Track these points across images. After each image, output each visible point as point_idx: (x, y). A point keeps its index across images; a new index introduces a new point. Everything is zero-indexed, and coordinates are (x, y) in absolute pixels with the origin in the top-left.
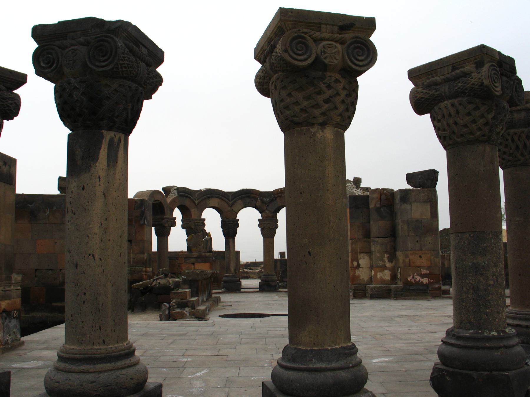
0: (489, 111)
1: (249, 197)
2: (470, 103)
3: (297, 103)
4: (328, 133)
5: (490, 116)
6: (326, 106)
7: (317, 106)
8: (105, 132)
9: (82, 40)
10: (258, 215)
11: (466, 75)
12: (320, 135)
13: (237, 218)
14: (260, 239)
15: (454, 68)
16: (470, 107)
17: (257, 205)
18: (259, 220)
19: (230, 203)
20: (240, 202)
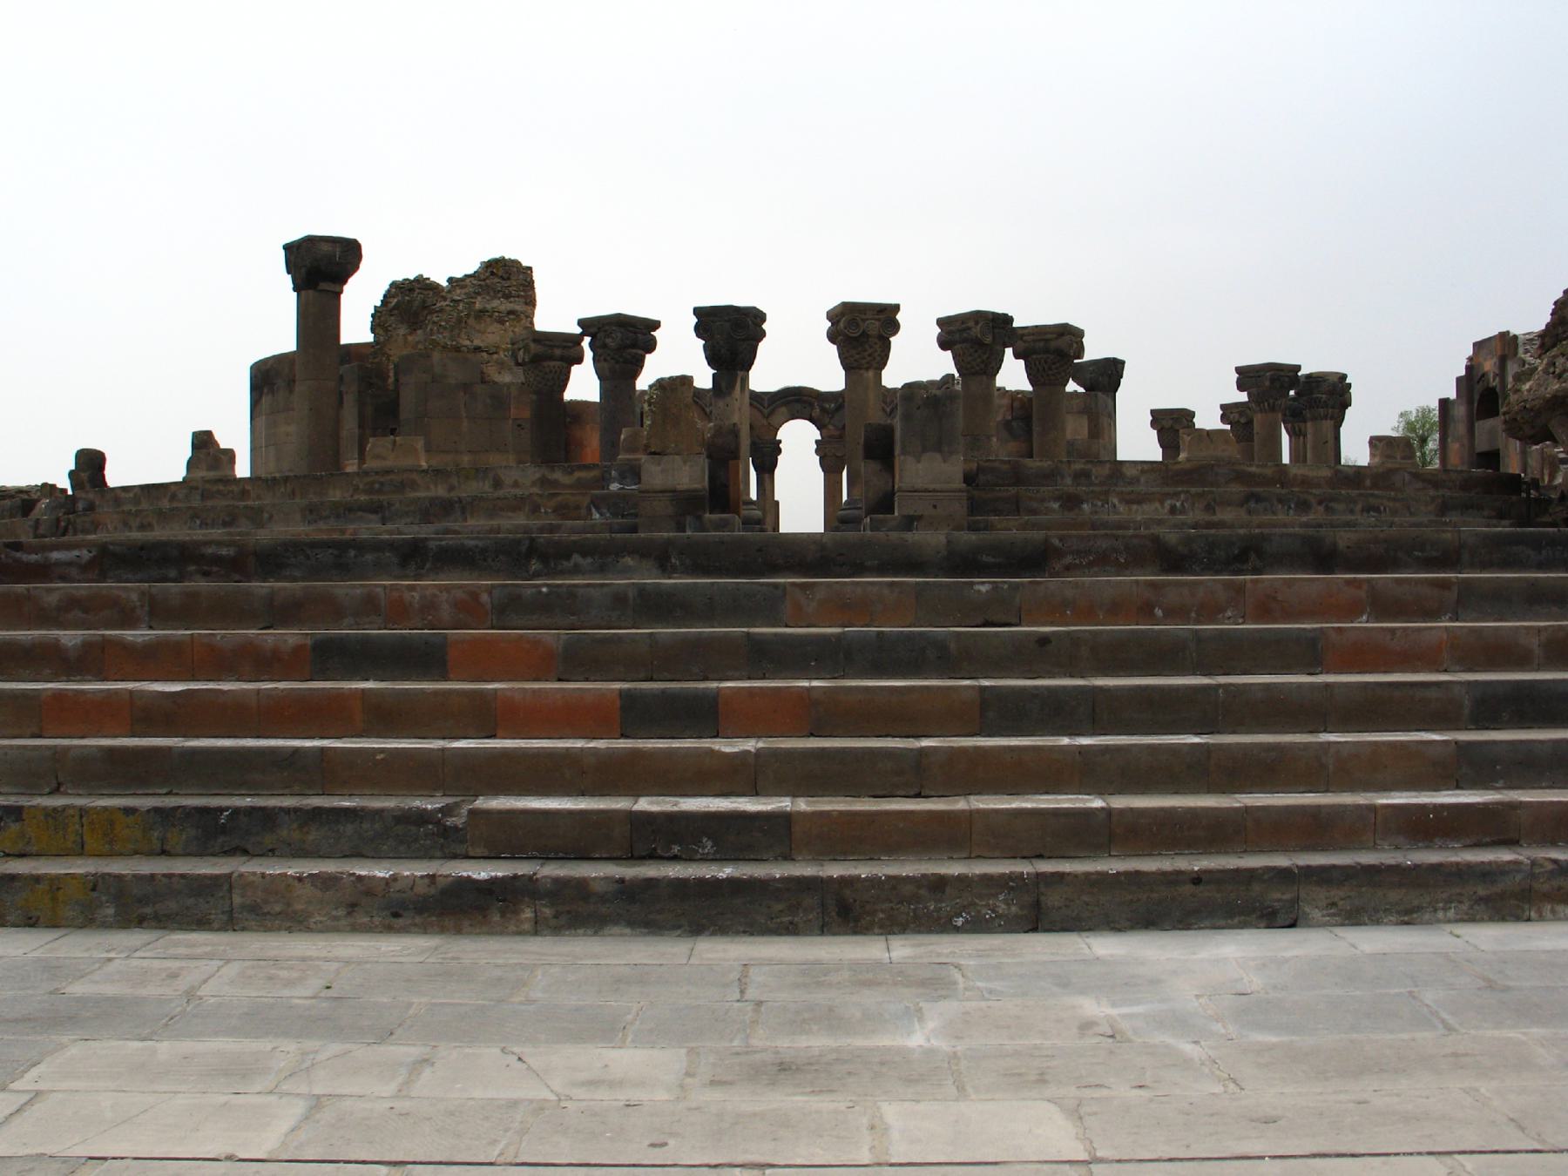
0: (985, 353)
1: (798, 401)
2: (972, 348)
3: (852, 356)
4: (871, 374)
5: (985, 357)
6: (869, 359)
7: (864, 358)
8: (739, 372)
9: (726, 318)
10: (815, 434)
11: (969, 328)
12: (865, 375)
13: (778, 438)
14: (819, 475)
15: (963, 323)
16: (971, 350)
17: (813, 414)
18: (817, 442)
19: (766, 411)
20: (783, 409)
